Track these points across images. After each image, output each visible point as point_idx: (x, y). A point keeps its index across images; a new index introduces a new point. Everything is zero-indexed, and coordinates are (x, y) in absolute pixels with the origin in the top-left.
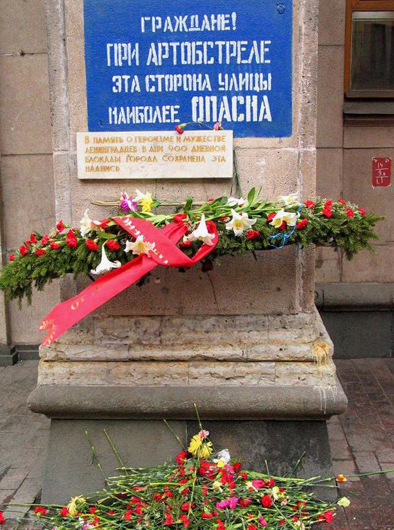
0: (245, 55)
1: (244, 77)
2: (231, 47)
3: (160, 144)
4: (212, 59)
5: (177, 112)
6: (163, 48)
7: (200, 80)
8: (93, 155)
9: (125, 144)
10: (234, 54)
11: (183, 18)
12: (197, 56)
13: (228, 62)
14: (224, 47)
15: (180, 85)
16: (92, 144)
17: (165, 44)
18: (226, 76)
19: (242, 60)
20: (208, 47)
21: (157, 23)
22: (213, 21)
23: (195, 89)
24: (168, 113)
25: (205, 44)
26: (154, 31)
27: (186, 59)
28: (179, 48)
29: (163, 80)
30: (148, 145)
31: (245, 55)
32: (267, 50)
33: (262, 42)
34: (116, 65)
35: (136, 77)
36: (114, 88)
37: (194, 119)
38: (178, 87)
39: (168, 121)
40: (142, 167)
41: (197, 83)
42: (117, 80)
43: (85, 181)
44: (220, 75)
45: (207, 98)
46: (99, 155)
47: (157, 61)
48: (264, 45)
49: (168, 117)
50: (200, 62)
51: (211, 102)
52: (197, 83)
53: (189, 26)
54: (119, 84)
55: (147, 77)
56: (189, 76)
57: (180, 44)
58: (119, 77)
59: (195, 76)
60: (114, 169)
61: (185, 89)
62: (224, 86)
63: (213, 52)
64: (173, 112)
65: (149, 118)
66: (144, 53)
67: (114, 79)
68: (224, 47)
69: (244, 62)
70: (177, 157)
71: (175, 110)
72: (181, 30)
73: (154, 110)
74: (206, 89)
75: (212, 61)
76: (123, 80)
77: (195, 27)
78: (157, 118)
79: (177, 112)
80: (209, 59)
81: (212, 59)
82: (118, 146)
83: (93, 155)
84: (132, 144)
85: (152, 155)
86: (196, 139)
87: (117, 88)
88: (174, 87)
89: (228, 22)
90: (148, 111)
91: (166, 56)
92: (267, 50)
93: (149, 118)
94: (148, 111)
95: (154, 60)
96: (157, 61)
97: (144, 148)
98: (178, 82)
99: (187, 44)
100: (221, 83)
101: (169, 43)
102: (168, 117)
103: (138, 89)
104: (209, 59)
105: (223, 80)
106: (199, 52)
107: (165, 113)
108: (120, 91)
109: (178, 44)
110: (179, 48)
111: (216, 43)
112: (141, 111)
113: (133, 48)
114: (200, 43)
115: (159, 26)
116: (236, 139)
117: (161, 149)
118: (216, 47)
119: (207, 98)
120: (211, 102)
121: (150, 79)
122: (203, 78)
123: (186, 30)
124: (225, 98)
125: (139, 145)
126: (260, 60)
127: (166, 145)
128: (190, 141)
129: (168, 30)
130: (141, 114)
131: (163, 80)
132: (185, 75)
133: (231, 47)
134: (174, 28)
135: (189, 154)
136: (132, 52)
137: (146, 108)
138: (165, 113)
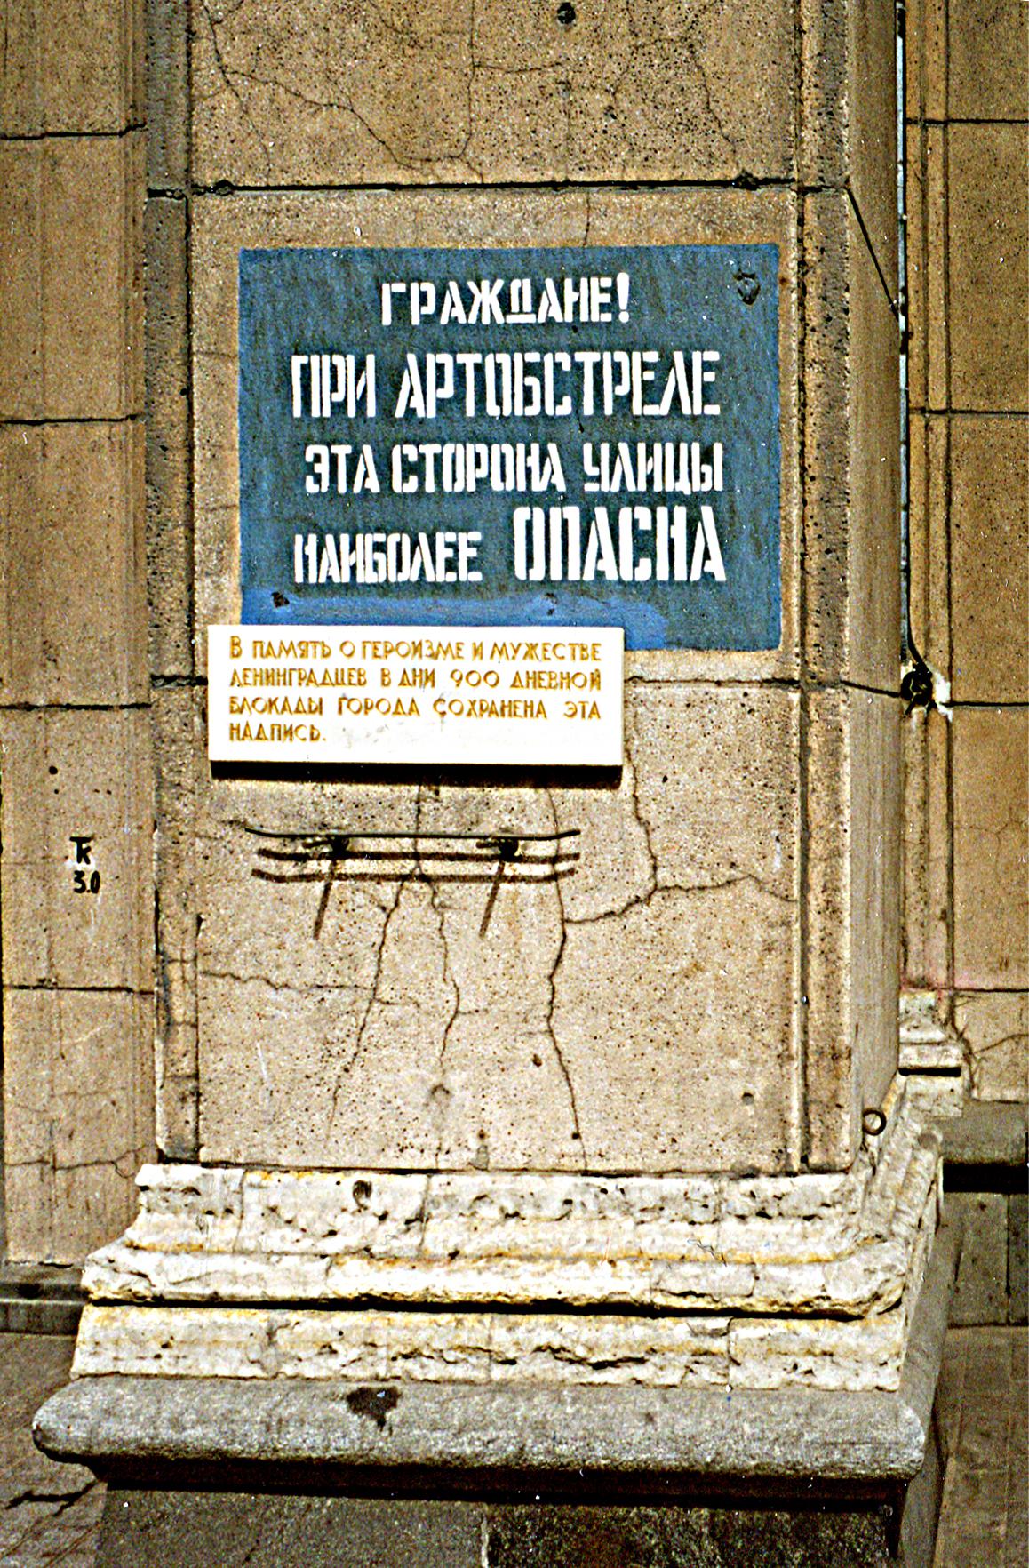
0: (652, 392)
1: (650, 453)
2: (617, 367)
4: (567, 400)
5: (473, 553)
6: (440, 368)
7: (534, 461)
8: (250, 692)
12: (528, 391)
13: (609, 409)
14: (598, 367)
15: (482, 473)
16: (248, 660)
17: (445, 358)
18: (605, 449)
19: (644, 403)
20: (557, 366)
23: (522, 487)
24: (450, 553)
25: (548, 358)
27: (499, 402)
28: (479, 369)
29: (438, 459)
31: (652, 392)
32: (710, 377)
33: (697, 358)
37: (520, 571)
39: (451, 577)
41: (528, 471)
42: (317, 458)
43: (226, 770)
44: (588, 449)
45: (555, 512)
47: (427, 410)
48: (704, 363)
49: (451, 565)
50: (533, 410)
51: (565, 523)
52: (528, 471)
53: (506, 309)
56: (507, 449)
57: (484, 358)
59: (521, 447)
60: (304, 732)
61: (497, 485)
62: (598, 479)
63: (568, 383)
64: (466, 553)
65: (399, 569)
66: (390, 382)
68: (598, 367)
69: (651, 410)
71: (470, 544)
72: (486, 320)
73: (415, 544)
74: (552, 487)
75: (566, 408)
76: (333, 459)
77: (521, 311)
78: (422, 570)
79: (473, 553)
80: (558, 401)
81: (567, 400)
83: (250, 692)
88: (467, 480)
91: (448, 391)
92: (710, 377)
93: (399, 569)
95: (417, 402)
96: (427, 410)
98: (478, 465)
99: (504, 358)
100: (590, 470)
101: (454, 353)
102: (451, 565)
104: (558, 401)
105: (596, 462)
106: (533, 381)
107: (443, 553)
108: (325, 489)
109: (477, 358)
110: (479, 369)
111: (579, 356)
112: (380, 547)
113: (360, 367)
114: (533, 357)
115: (430, 309)
116: (630, 654)
118: (578, 367)
119: (555, 512)
120: (565, 523)
121: (404, 458)
122: (544, 455)
123: (500, 319)
124: (601, 513)
125: (372, 668)
126: (692, 406)
129: (453, 321)
130: (380, 556)
131: (438, 459)
133: (617, 367)
134: (467, 317)
136: (357, 378)
137: (393, 539)
138: (443, 553)
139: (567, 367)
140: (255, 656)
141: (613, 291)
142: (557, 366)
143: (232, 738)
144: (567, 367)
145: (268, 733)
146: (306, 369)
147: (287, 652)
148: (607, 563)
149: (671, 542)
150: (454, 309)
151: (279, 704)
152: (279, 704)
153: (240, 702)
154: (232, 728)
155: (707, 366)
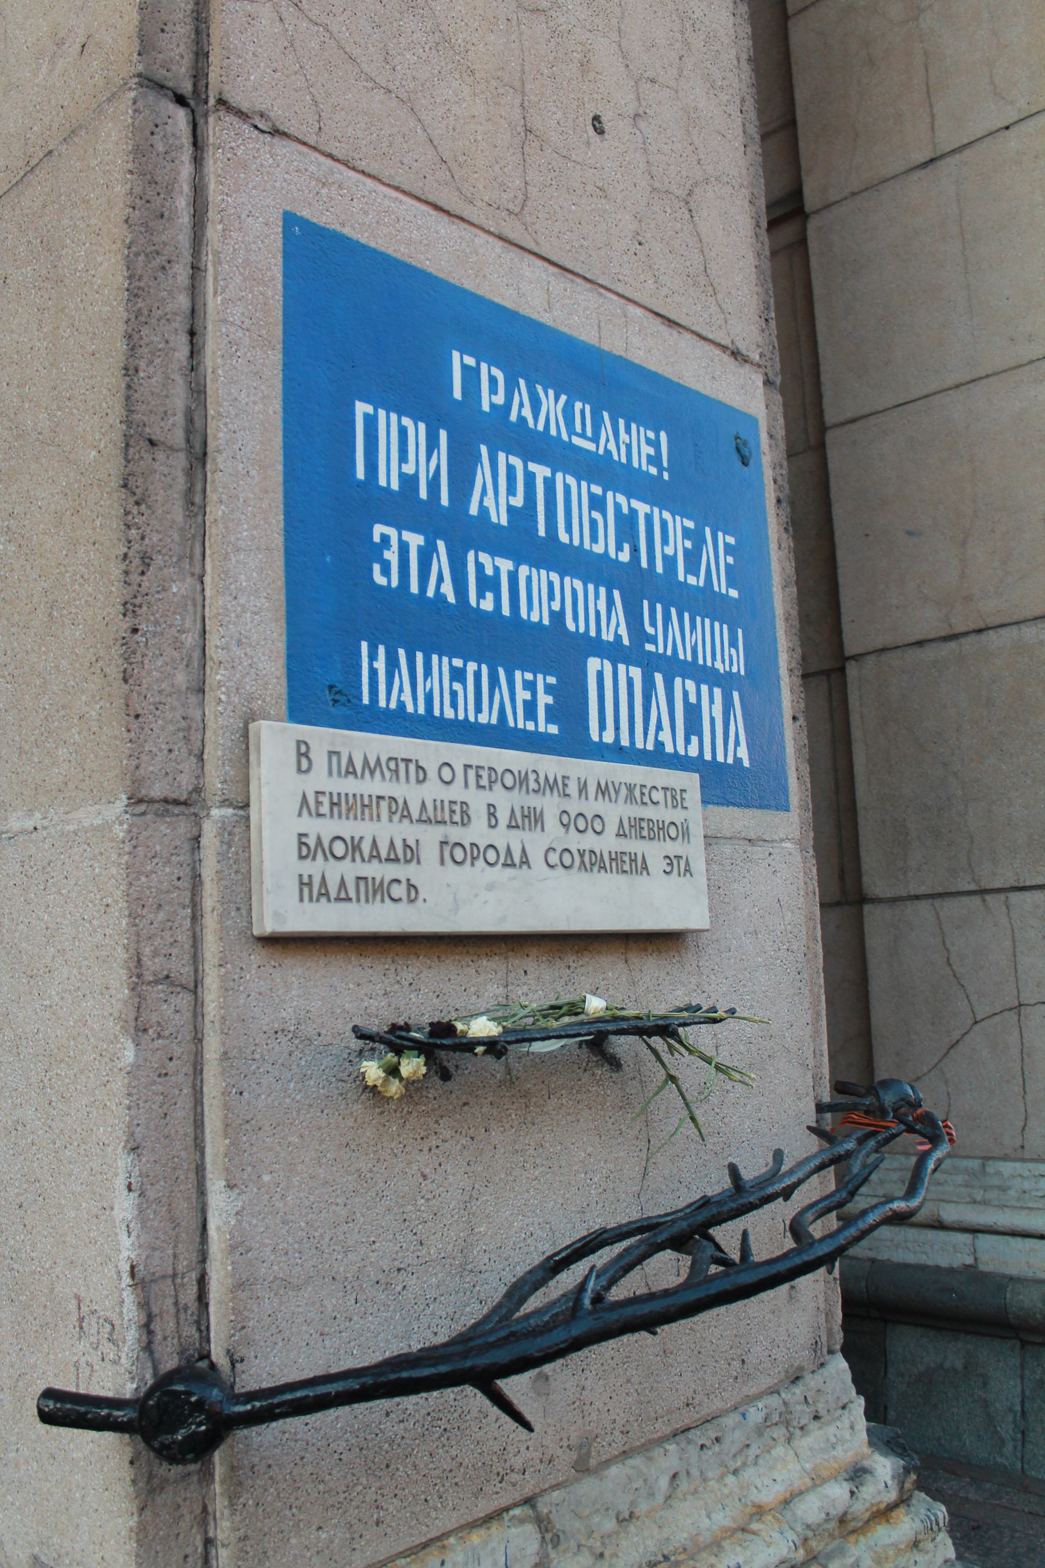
3: (535, 801)
4: (626, 547)
8: (326, 828)
9: (432, 791)
10: (669, 551)
11: (557, 399)
16: (319, 779)
20: (617, 507)
21: (493, 390)
22: (623, 436)
26: (486, 407)
30: (504, 801)
34: (383, 482)
35: (441, 545)
36: (377, 568)
38: (552, 613)
40: (491, 887)
46: (348, 828)
53: (571, 432)
54: (392, 556)
55: (471, 556)
58: (392, 532)
67: (379, 530)
70: (581, 854)
75: (625, 557)
82: (413, 794)
84: (456, 792)
85: (515, 840)
86: (624, 791)
87: (386, 571)
89: (651, 451)
90: (478, 675)
94: (478, 675)
97: (492, 811)
103: (448, 589)
117: (534, 819)
127: (550, 805)
128: (610, 800)
132: (567, 579)
133: (664, 524)
135: (608, 843)
139: (625, 510)
140: (330, 773)
141: (656, 444)
142: (617, 507)
143: (301, 900)
144: (625, 510)
145: (352, 894)
146: (371, 422)
147: (372, 773)
148: (665, 736)
149: (712, 720)
150: (521, 409)
151: (366, 847)
152: (366, 847)
153: (312, 842)
154: (302, 883)
155: (729, 549)
